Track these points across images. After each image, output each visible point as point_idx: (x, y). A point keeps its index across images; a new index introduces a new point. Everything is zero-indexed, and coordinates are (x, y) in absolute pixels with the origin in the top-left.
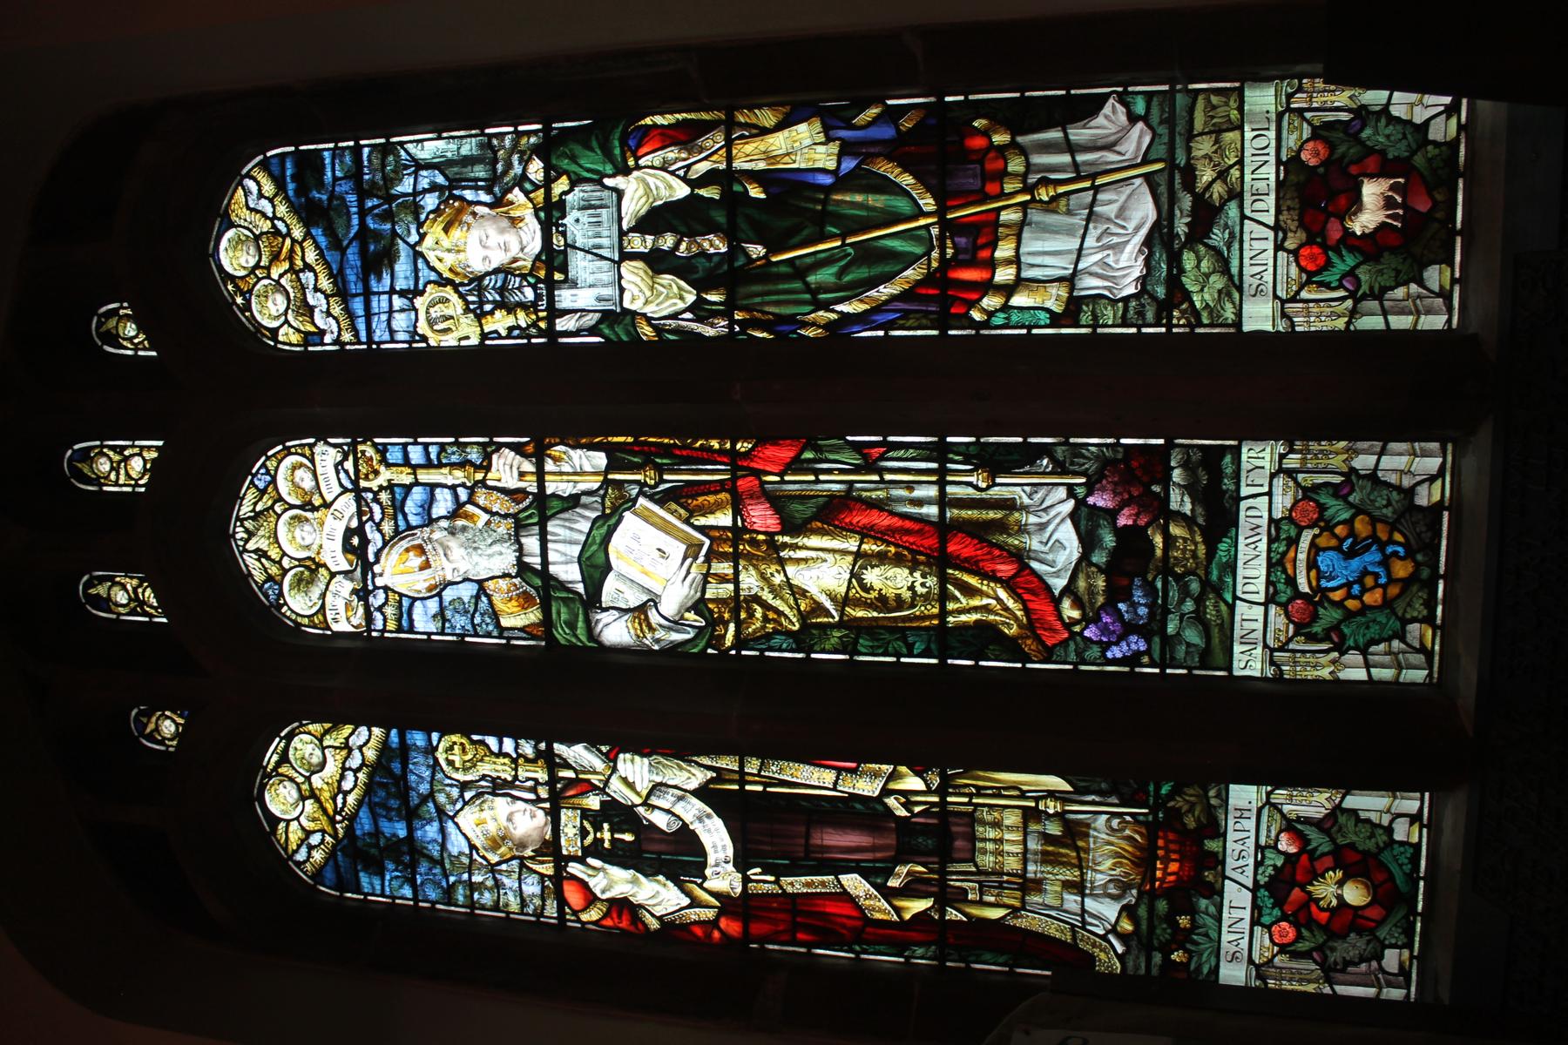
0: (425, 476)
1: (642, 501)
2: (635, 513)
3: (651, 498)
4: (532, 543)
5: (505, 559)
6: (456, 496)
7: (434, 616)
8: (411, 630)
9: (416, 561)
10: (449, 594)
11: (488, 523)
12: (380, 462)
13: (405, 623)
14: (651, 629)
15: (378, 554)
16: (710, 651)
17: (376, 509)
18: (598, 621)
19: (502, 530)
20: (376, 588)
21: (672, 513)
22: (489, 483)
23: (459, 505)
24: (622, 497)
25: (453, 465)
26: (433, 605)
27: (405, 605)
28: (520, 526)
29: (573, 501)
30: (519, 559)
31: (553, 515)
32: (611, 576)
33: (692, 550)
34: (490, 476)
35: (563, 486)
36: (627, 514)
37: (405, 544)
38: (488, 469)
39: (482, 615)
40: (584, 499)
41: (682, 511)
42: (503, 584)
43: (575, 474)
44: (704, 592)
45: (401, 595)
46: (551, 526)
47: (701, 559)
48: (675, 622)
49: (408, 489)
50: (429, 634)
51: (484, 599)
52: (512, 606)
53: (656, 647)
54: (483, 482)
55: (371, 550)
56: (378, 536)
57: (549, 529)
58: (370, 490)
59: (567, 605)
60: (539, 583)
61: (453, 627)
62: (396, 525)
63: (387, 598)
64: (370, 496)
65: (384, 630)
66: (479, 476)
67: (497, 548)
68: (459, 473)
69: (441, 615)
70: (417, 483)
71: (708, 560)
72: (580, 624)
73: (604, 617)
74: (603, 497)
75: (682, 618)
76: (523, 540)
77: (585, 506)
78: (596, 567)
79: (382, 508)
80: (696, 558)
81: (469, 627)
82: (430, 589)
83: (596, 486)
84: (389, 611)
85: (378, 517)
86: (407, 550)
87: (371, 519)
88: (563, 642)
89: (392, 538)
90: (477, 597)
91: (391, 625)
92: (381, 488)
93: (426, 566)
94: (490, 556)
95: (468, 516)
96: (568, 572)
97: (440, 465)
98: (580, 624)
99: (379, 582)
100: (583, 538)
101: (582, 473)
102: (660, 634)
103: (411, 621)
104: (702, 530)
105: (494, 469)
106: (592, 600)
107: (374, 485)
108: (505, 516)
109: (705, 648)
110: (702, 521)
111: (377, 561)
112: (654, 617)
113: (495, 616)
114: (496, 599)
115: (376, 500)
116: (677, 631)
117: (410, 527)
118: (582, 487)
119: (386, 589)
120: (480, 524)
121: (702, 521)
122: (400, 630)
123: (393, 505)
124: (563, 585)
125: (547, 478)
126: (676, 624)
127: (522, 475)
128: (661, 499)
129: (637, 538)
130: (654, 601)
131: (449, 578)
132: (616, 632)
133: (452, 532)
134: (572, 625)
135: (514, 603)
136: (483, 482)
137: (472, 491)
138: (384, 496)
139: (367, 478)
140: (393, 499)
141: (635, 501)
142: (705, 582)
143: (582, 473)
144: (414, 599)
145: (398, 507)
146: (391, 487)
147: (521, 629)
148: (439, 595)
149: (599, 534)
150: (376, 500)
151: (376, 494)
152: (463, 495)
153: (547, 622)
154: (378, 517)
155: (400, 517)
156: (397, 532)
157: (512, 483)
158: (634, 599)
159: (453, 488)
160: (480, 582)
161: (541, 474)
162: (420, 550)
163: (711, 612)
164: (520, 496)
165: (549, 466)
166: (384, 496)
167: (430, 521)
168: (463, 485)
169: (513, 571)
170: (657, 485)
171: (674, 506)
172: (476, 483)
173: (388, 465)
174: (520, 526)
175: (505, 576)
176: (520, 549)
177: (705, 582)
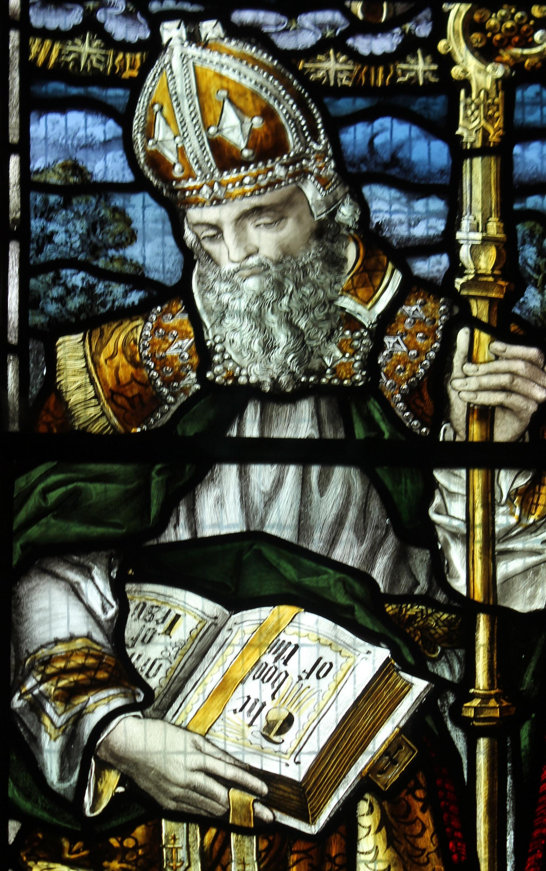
0: (477, 177)
1: (420, 685)
2: (385, 670)
3: (425, 709)
4: (300, 423)
5: (248, 349)
6: (426, 248)
7: (74, 168)
8: (35, 105)
9: (234, 130)
10: (144, 211)
11: (350, 321)
12: (517, 64)
13: (56, 87)
14: (68, 696)
15: (252, 34)
16: (13, 828)
17: (383, 44)
18: (87, 573)
19: (333, 354)
20: (155, 22)
21: (391, 750)
22: (463, 336)
23: (405, 253)
24: (430, 642)
25: (508, 250)
26: (110, 167)
27: (113, 91)
28: (340, 400)
29: (415, 531)
30: (253, 391)
31: (372, 481)
32: (212, 608)
33: (281, 792)
34: (483, 337)
35: (457, 508)
36: (382, 653)
37: (286, 109)
38: (499, 332)
39: (88, 290)
40: (420, 560)
41: (393, 775)
42: (180, 348)
43: (490, 538)
44: (176, 816)
45: (135, 86)
46: (341, 485)
47: (266, 814)
48: (91, 749)
49: (443, 127)
50: (23, 148)
51: (135, 297)
52: (115, 364)
53: (17, 703)
54: (461, 317)
55: (268, 20)
56: (307, 39)
57: (339, 473)
58: (440, 31)
59: (127, 497)
60: (194, 427)
61: (48, 213)
62: (340, 92)
63: (124, 46)
64: (423, 31)
65: (28, 32)
66: (479, 310)
67: (282, 337)
68: (487, 261)
69: (78, 185)
70: (460, 153)
71: (261, 829)
72: (76, 529)
73: (97, 590)
74: (426, 599)
75: (103, 766)
76: (305, 408)
77: (401, 560)
78: (240, 572)
79: (386, 60)
80: (267, 801)
81: (50, 253)
82: (156, 160)
83: (459, 585)
84: (87, 49)
85: (363, 45)
86: (268, 114)
87: (357, 28)
88: (21, 483)
89: (302, 76)
90: (136, 278)
91: (39, 50)
92: (447, 61)
93: (225, 157)
94: (259, 320)
95: (367, 280)
96: (219, 508)
97: (509, 217)
98: (76, 529)
99: (172, 32)
100: (316, 545)
101: (491, 557)
102: (54, 714)
103: (63, 105)
104: (345, 821)
105: (498, 346)
106: (143, 557)
107: (454, 43)
108: (371, 364)
109: (19, 815)
110: (367, 819)
111: (234, 31)
112: (101, 704)
113: (92, 321)
114: (139, 330)
115: (409, 46)
116: (66, 755)
117: (335, 126)
118: (456, 554)
119: (154, 48)
120: (348, 303)
121: (367, 819)
122: (31, 72)
123: (394, 88)
124: (185, 490)
125: (478, 478)
126: (87, 752)
127: (486, 414)
128: (423, 727)
129: (319, 669)
130: (150, 703)
131: (194, 214)
132: (60, 612)
133: (325, 232)
134: (71, 506)
135: (127, 372)
136: (461, 317)
137: (439, 289)
138: (420, 67)
139: (470, 26)
140: (412, 87)
141: (420, 672)
142: (205, 821)
143: (491, 557)
144: (124, 118)
145: (396, 100)
146: (449, 86)
147: (51, 386)
148: (140, 184)
149: (327, 580)
150: (409, 46)
151: (429, 46)
152: (432, 266)
153: (74, 445)
154: (363, 45)
155: (361, 103)
156: (319, 92)
157: (466, 387)
158: (154, 656)
159: (447, 243)
160: (181, 292)
161: (485, 456)
162: (268, 146)
163: (125, 831)
164: (428, 406)
165: (507, 481)
166: (420, 67)
167: (354, 176)
168: (456, 268)
169: (217, 374)
170: (462, 723)
171: (406, 758)
172: (464, 303)
173: (507, 86)
174: (340, 400)
175: (204, 354)
176: (275, 397)
177: (205, 821)
